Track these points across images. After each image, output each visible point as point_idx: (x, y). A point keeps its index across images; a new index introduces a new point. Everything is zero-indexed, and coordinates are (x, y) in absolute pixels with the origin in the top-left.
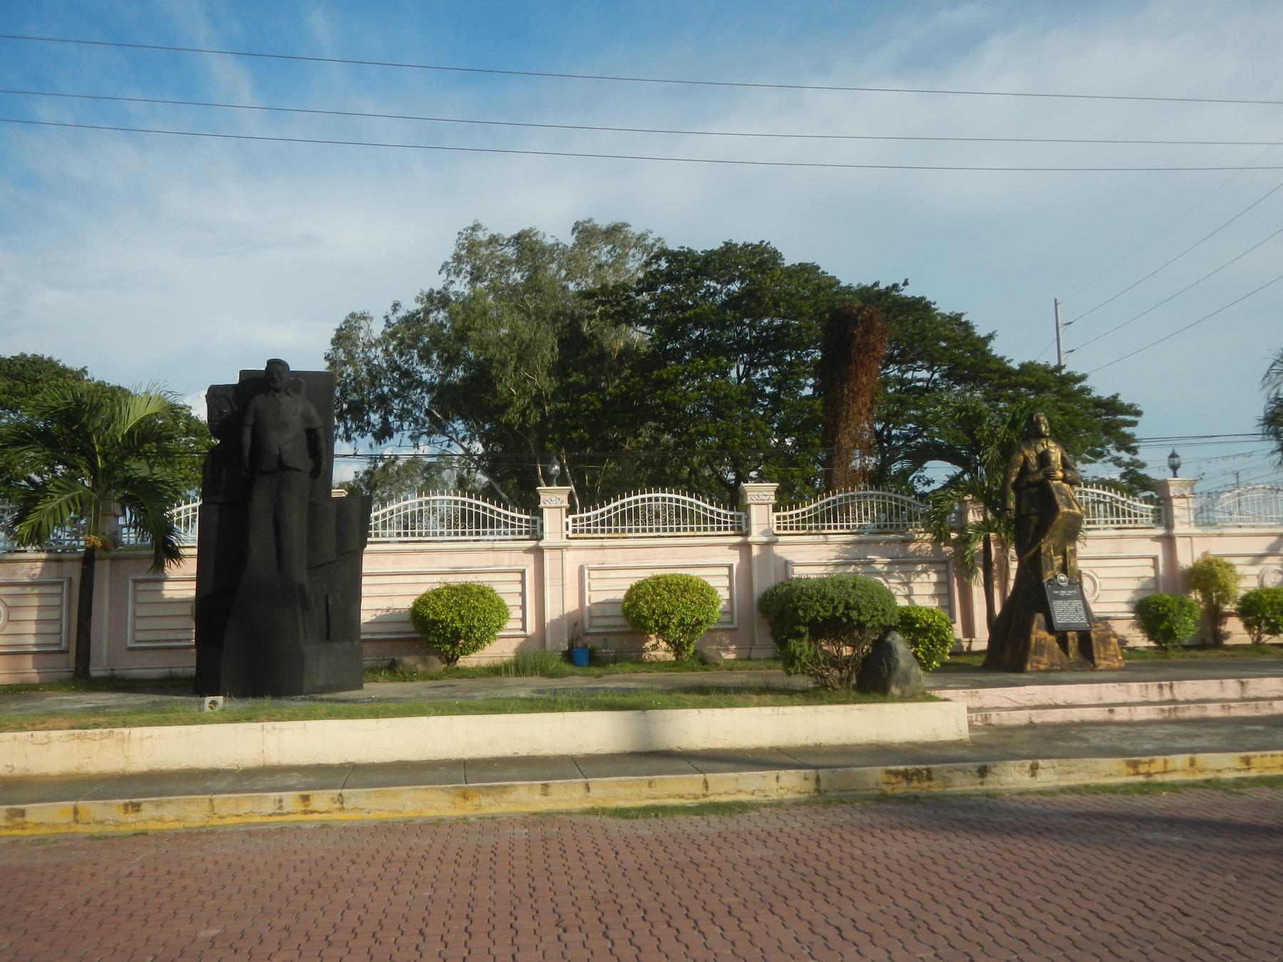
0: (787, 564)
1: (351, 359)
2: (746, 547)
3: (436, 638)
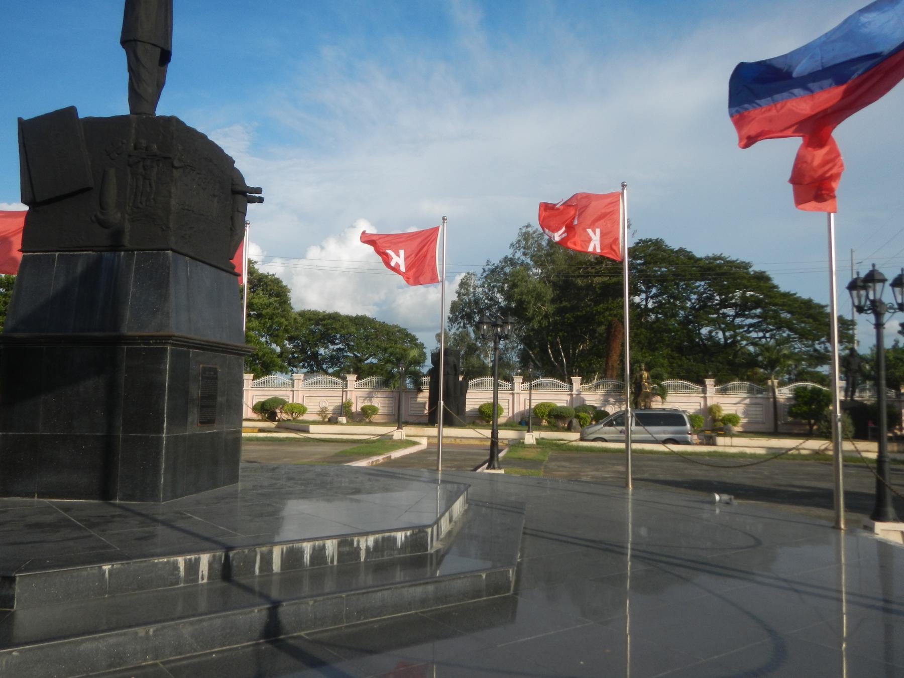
0: (584, 400)
1: (467, 294)
2: (571, 395)
3: (486, 416)
